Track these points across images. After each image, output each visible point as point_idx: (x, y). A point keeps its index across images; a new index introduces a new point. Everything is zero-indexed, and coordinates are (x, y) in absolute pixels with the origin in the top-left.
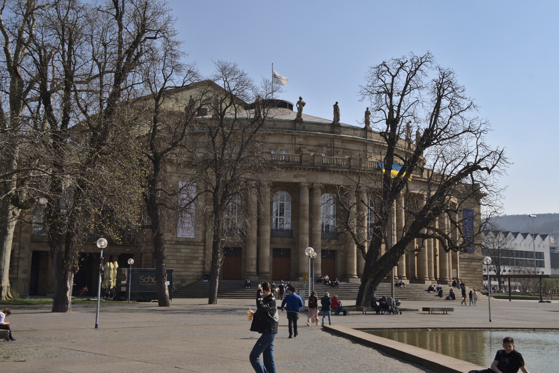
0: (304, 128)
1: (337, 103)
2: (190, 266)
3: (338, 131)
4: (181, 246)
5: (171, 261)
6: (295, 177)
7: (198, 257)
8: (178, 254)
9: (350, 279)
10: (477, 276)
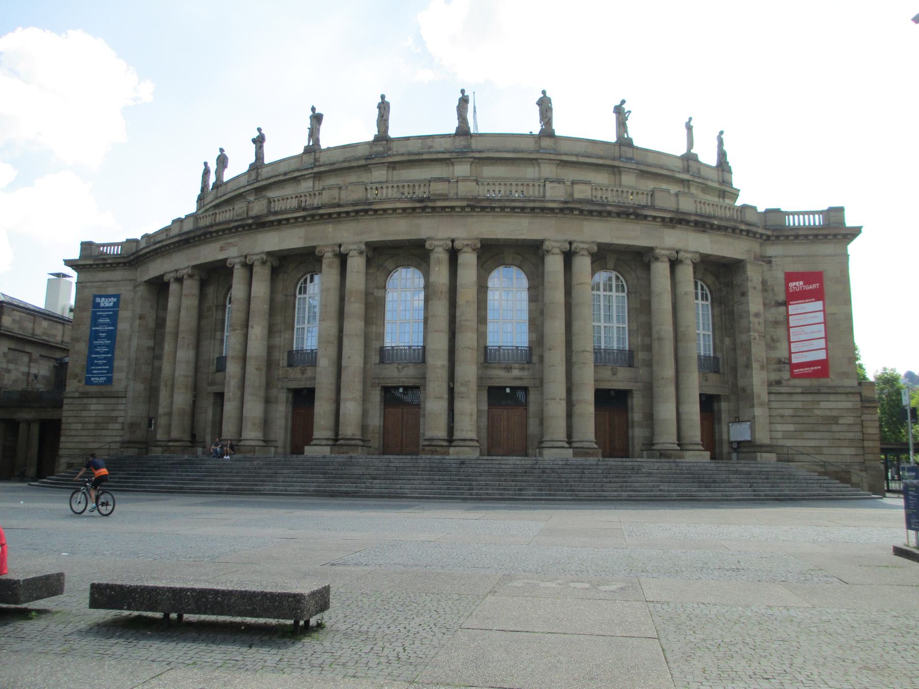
0: (316, 160)
1: (383, 97)
2: (104, 432)
3: (381, 149)
4: (91, 399)
5: (74, 426)
6: (222, 249)
7: (117, 417)
8: (84, 414)
9: (306, 448)
10: (837, 436)
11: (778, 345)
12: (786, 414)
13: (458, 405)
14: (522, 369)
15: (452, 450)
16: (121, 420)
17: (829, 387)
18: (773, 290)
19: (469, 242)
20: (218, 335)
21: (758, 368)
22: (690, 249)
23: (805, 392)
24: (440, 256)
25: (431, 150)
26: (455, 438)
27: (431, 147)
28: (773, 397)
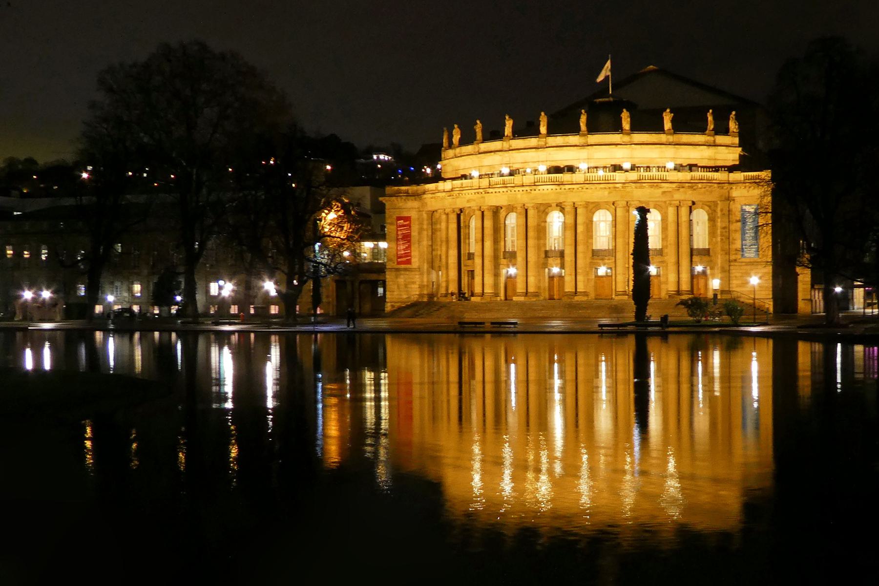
11: (736, 241)
13: (579, 278)
14: (609, 259)
15: (576, 297)
16: (418, 283)
19: (581, 203)
20: (467, 242)
24: (569, 209)
27: (568, 143)
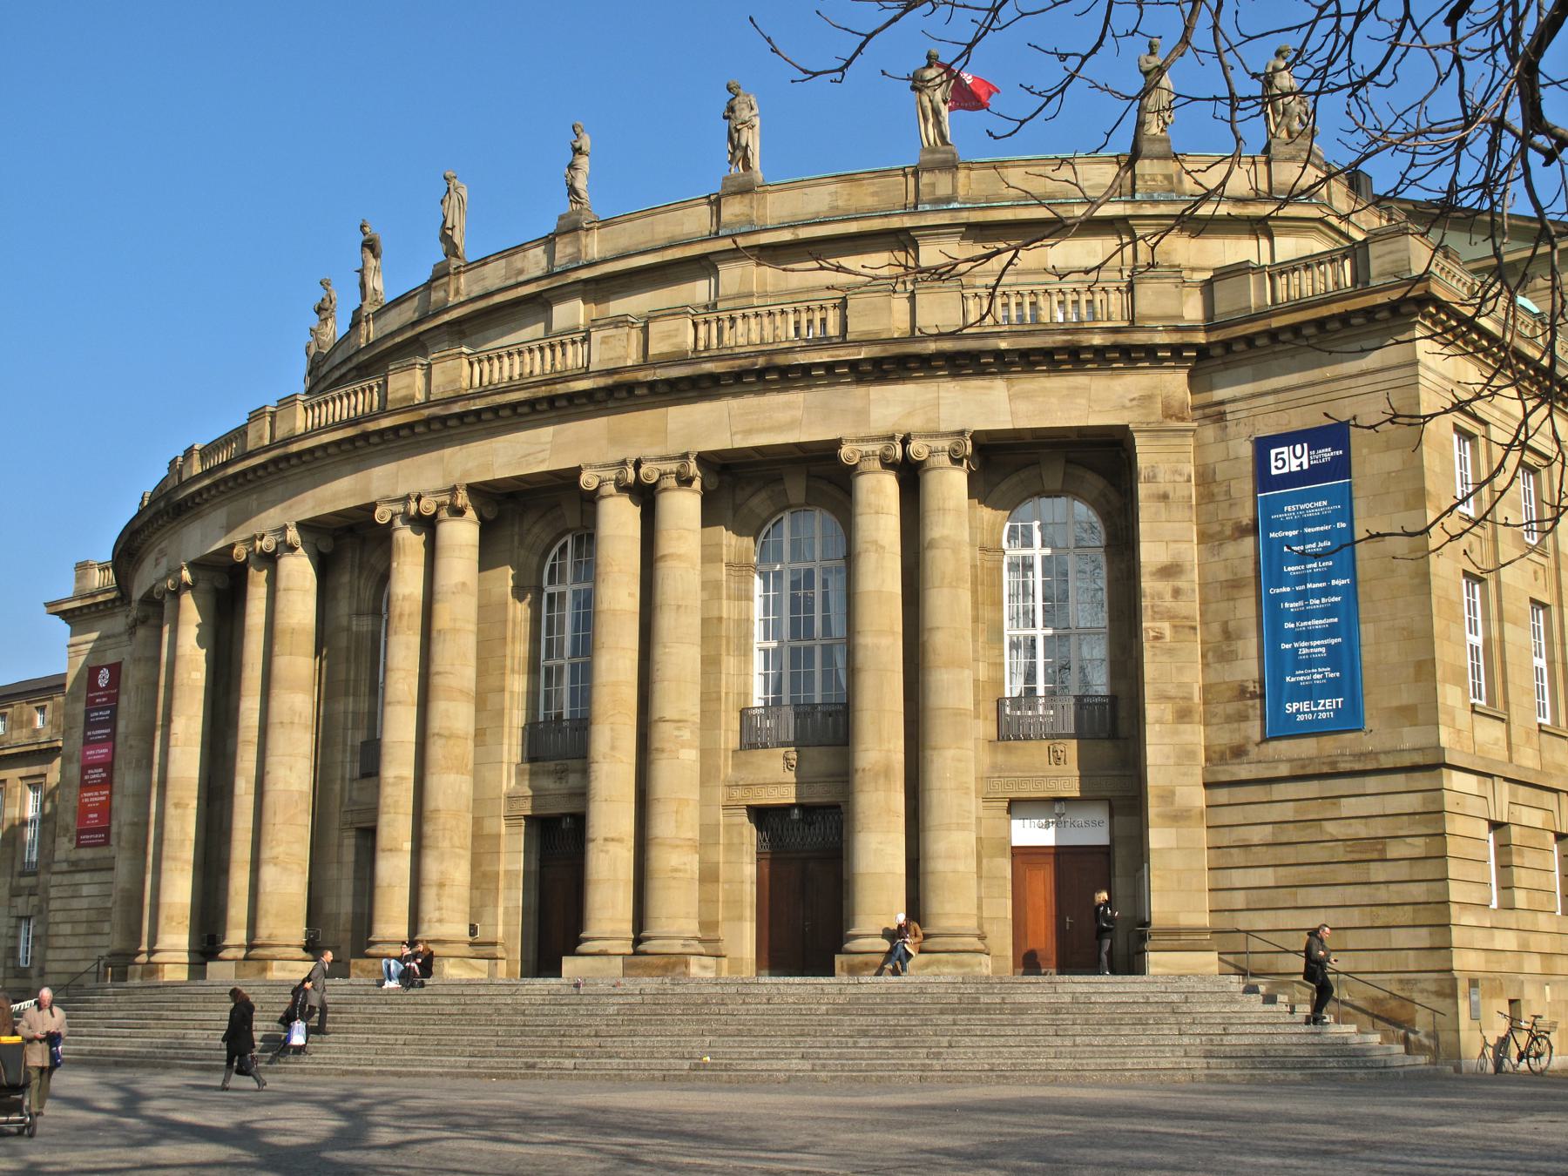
10: (1383, 894)
11: (1239, 645)
12: (1256, 840)
13: (432, 867)
17: (1360, 756)
18: (1228, 492)
21: (1169, 716)
22: (944, 428)
23: (1300, 772)
25: (521, 278)
26: (419, 937)
27: (521, 272)
28: (1222, 795)
